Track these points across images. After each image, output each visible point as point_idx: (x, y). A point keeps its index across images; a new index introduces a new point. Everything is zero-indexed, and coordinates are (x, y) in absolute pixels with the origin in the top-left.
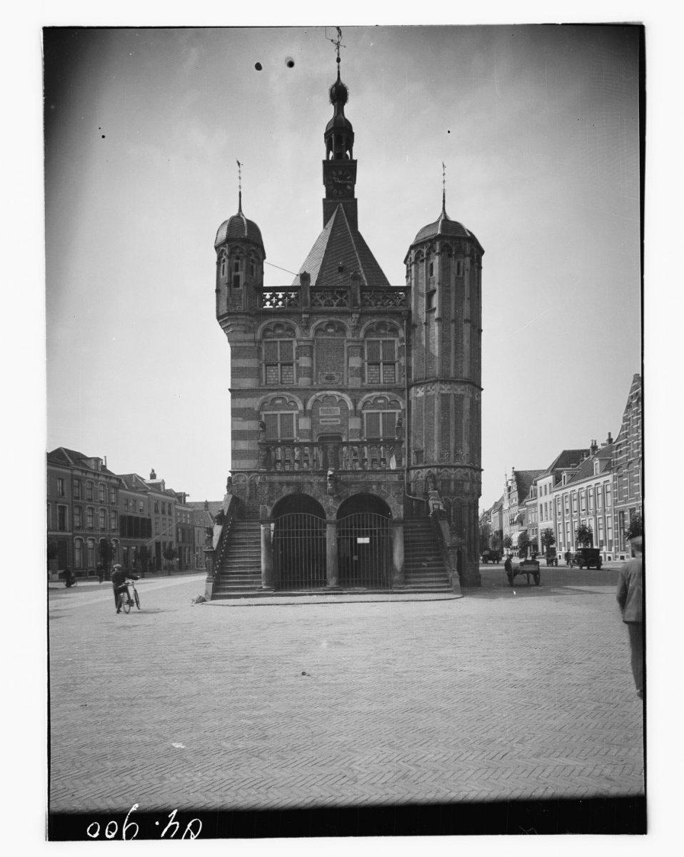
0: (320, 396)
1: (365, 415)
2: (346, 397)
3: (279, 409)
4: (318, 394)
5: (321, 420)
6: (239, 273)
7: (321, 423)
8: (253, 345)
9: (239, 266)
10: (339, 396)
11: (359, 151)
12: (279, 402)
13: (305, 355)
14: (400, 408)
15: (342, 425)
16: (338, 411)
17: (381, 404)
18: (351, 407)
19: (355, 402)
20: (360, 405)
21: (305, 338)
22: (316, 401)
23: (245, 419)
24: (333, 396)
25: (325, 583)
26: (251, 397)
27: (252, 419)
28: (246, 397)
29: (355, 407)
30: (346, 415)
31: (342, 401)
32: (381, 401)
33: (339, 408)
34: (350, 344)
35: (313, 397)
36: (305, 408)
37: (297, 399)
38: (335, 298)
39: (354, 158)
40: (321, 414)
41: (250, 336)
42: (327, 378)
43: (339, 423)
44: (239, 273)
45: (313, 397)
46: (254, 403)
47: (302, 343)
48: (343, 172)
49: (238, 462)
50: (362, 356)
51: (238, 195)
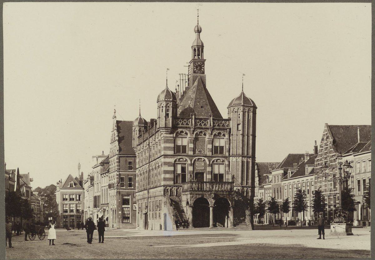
2: (206, 159)
4: (196, 158)
5: (197, 167)
6: (168, 113)
7: (196, 168)
8: (172, 138)
9: (169, 110)
11: (206, 55)
15: (204, 169)
18: (208, 163)
19: (210, 161)
21: (192, 137)
24: (201, 159)
25: (209, 226)
26: (171, 158)
27: (172, 166)
29: (210, 163)
31: (204, 160)
33: (203, 163)
37: (188, 159)
38: (203, 122)
39: (204, 58)
40: (197, 165)
41: (172, 135)
42: (199, 152)
43: (203, 169)
44: (168, 113)
45: (194, 159)
46: (172, 160)
48: (200, 63)
49: (166, 182)
51: (166, 80)
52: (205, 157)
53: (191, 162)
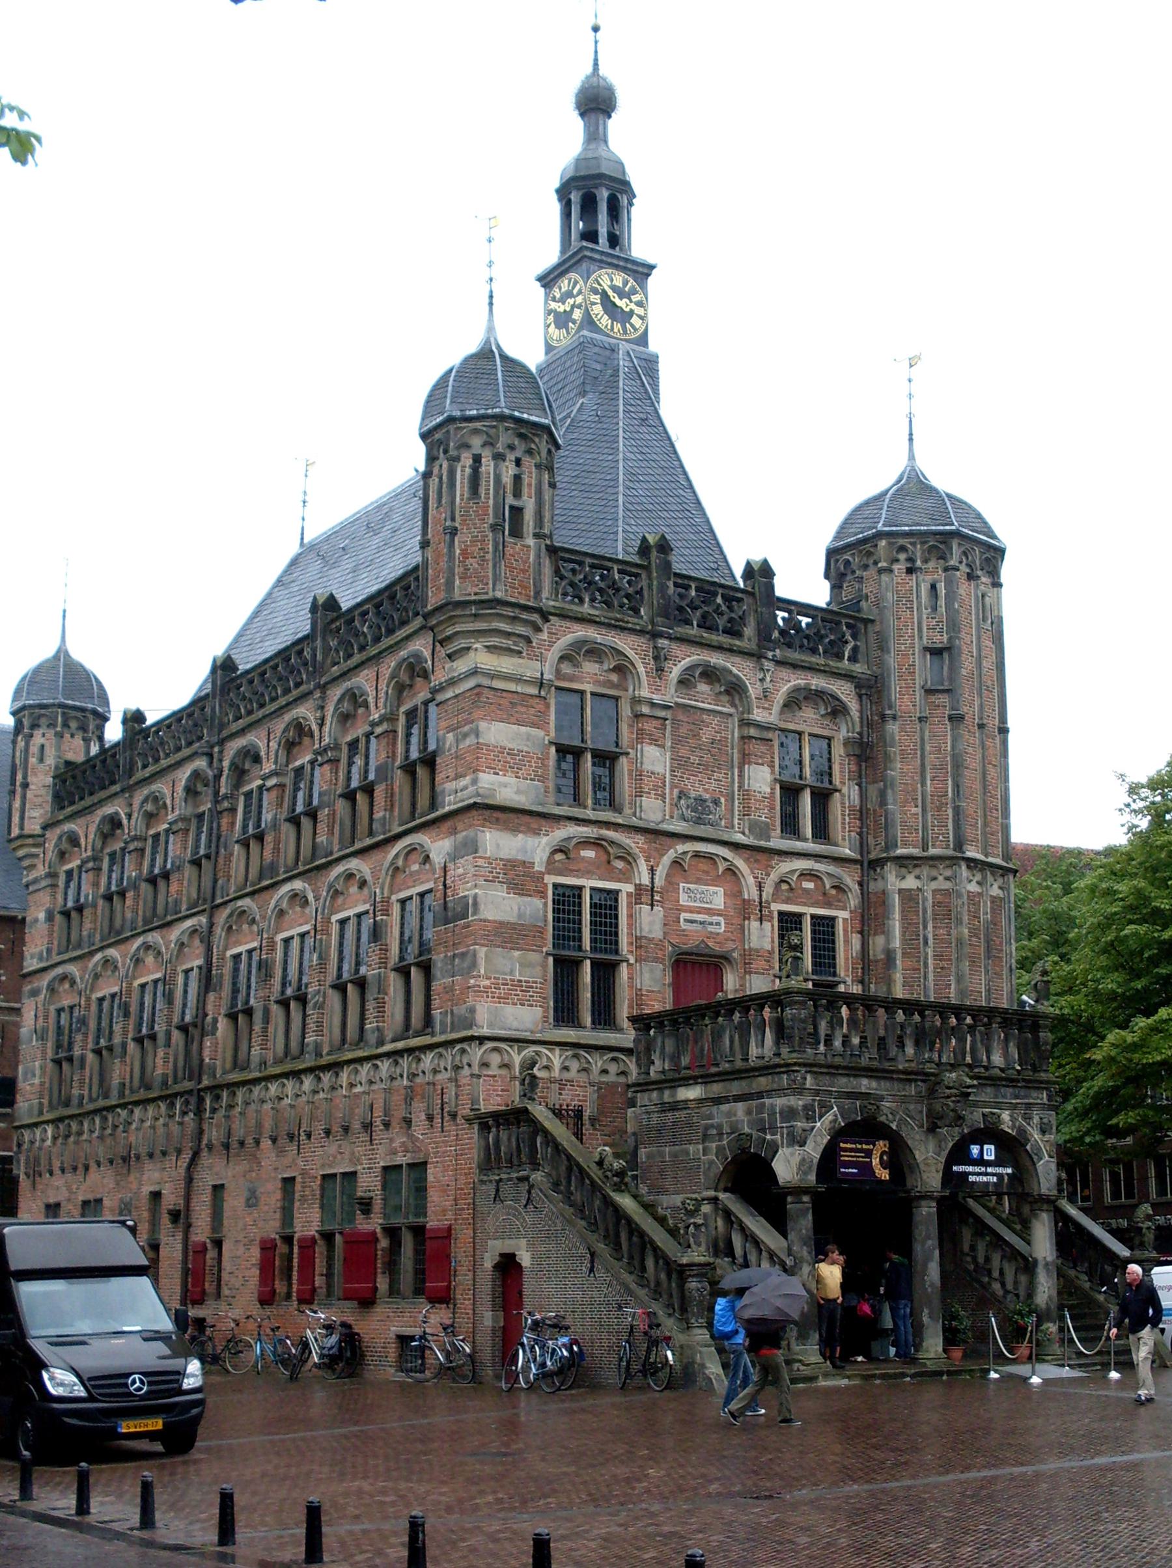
0: (685, 853)
1: (776, 915)
2: (740, 863)
3: (588, 874)
4: (681, 848)
5: (683, 916)
10: (725, 859)
12: (589, 854)
13: (654, 742)
14: (844, 909)
16: (717, 897)
17: (806, 890)
20: (768, 890)
21: (657, 698)
22: (676, 863)
23: (517, 888)
24: (710, 858)
28: (515, 830)
30: (744, 910)
31: (731, 871)
32: (810, 885)
33: (721, 891)
34: (753, 732)
35: (671, 855)
36: (653, 883)
40: (683, 900)
41: (529, 668)
47: (645, 710)
50: (772, 766)
52: (735, 846)
53: (653, 883)
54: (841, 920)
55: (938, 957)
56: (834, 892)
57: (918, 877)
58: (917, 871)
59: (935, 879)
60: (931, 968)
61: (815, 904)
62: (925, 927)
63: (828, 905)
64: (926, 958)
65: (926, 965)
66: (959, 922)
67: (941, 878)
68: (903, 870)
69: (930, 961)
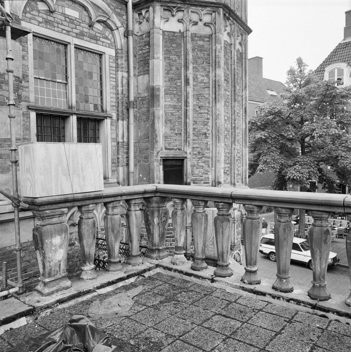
17: (72, 21)
54: (107, 57)
55: (198, 97)
56: (99, 27)
57: (180, 21)
58: (180, 15)
59: (196, 24)
60: (191, 108)
61: (80, 35)
62: (186, 67)
63: (95, 39)
64: (187, 97)
65: (186, 102)
66: (216, 65)
67: (200, 24)
68: (167, 13)
69: (191, 100)
